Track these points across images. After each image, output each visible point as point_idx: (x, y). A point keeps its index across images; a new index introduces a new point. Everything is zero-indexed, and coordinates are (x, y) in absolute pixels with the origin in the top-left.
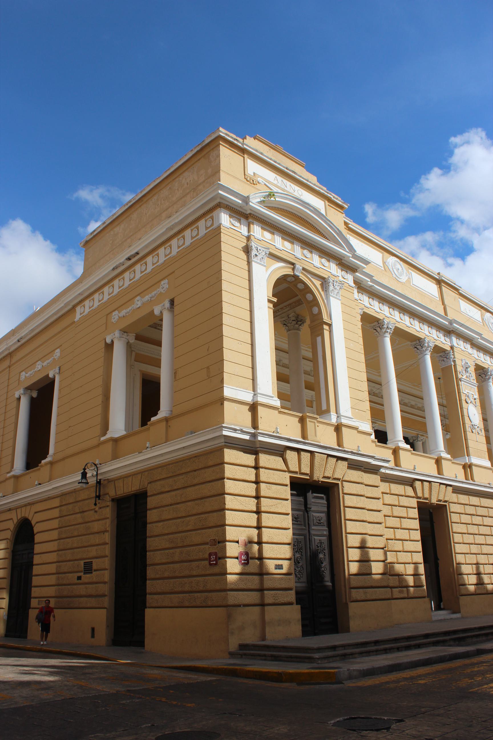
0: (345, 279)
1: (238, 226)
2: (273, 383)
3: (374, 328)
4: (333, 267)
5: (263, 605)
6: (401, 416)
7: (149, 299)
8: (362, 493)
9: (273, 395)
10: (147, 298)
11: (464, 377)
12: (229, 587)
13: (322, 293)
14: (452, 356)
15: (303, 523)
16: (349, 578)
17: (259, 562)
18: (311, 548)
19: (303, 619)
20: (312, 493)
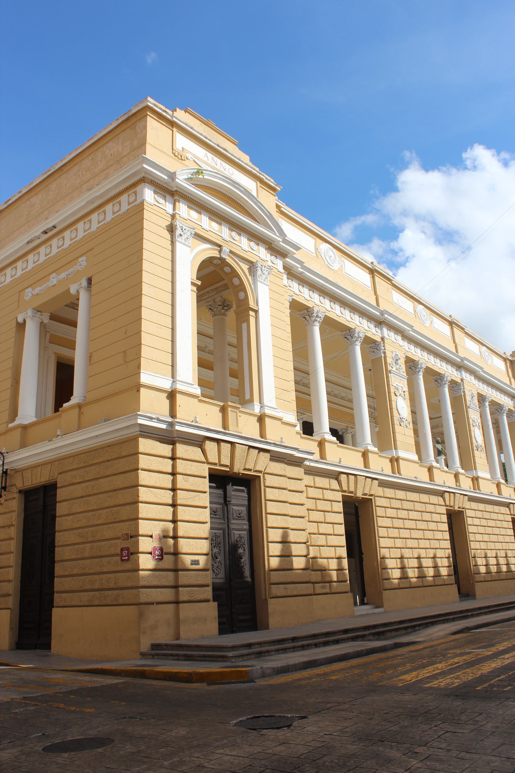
0: (274, 264)
1: (163, 203)
2: (193, 370)
3: (303, 316)
4: (262, 251)
5: (177, 602)
6: (328, 407)
7: (65, 276)
8: (285, 487)
9: (193, 383)
10: (63, 275)
11: (394, 369)
12: (142, 583)
13: (250, 278)
14: (383, 348)
15: (221, 517)
16: (269, 574)
17: (174, 558)
18: (230, 542)
19: (220, 617)
20: (232, 486)
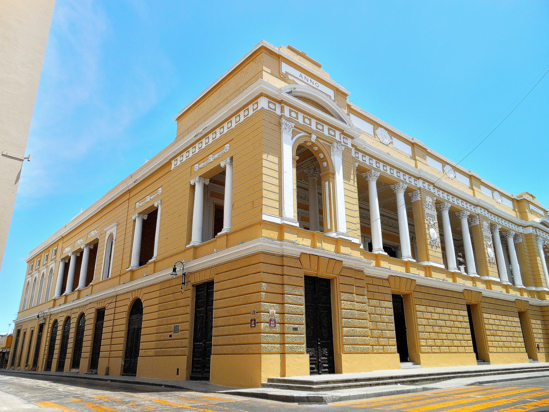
10: (216, 156)
